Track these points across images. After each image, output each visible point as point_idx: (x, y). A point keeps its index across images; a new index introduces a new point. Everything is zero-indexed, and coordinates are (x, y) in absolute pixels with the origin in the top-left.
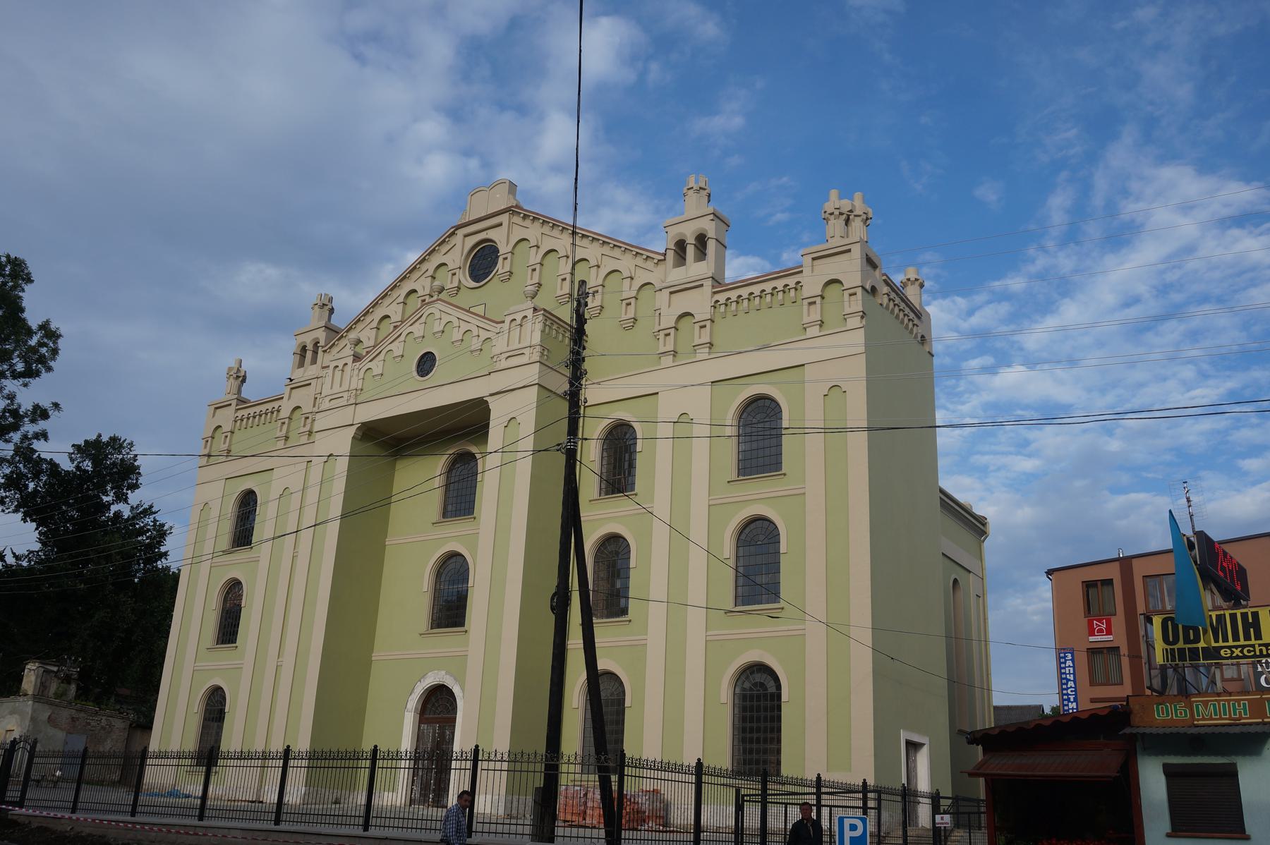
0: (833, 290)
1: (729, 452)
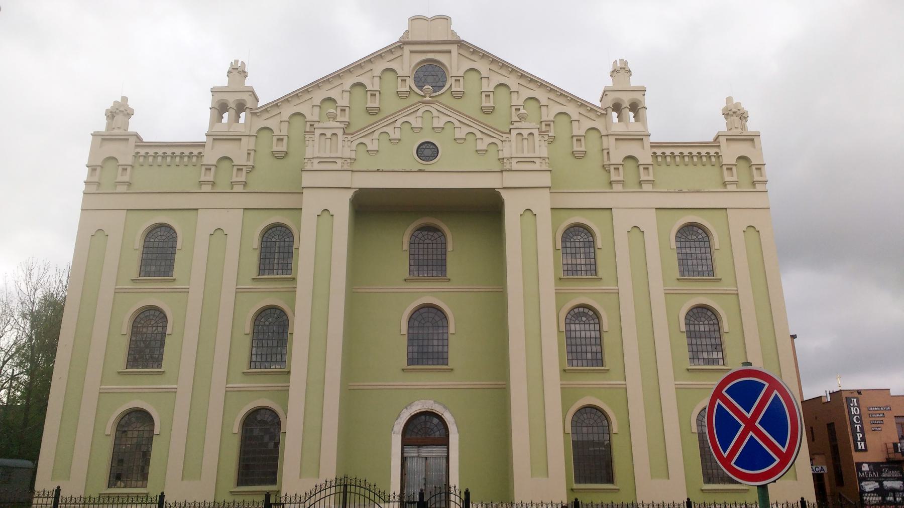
0: (226, 164)
1: (253, 259)
